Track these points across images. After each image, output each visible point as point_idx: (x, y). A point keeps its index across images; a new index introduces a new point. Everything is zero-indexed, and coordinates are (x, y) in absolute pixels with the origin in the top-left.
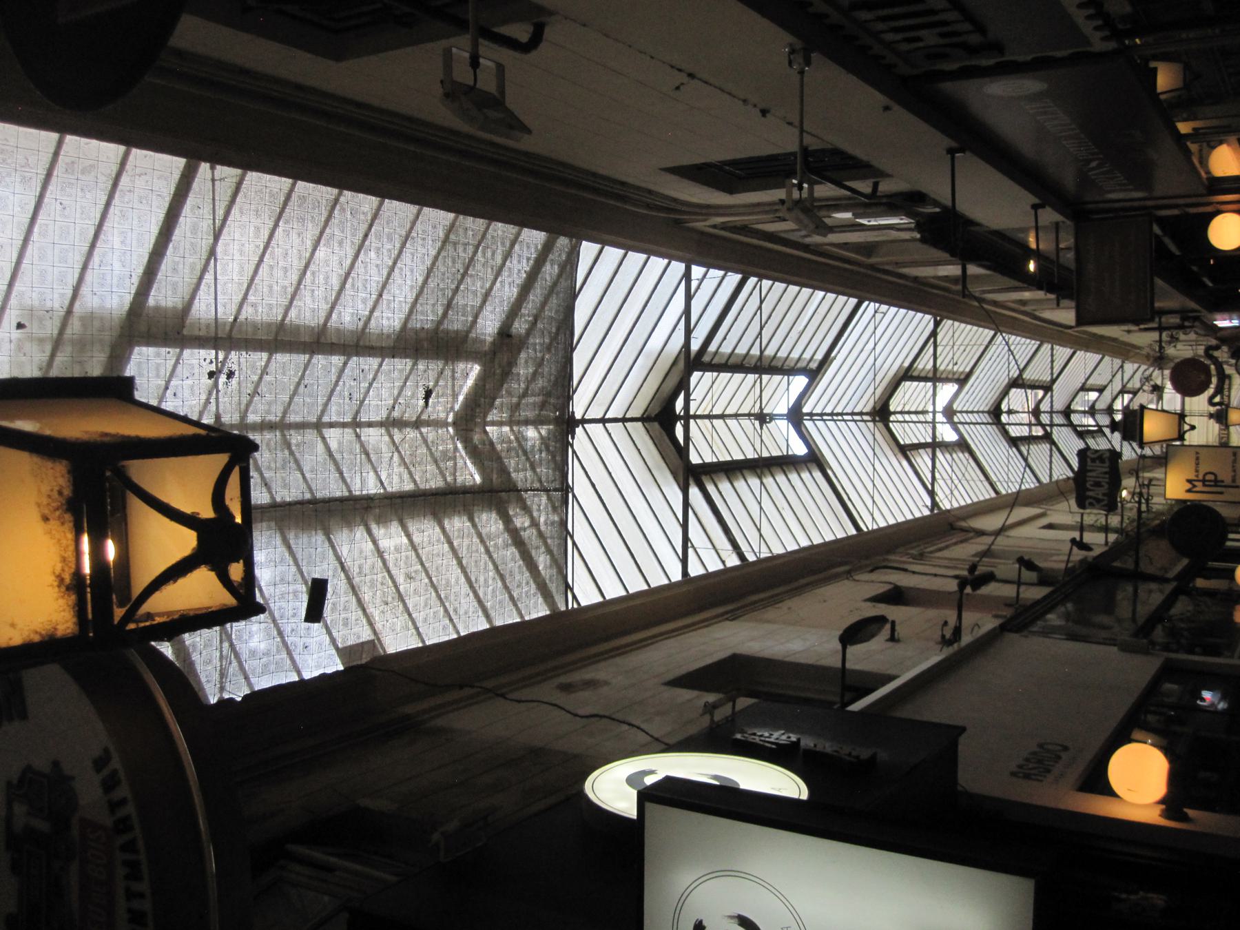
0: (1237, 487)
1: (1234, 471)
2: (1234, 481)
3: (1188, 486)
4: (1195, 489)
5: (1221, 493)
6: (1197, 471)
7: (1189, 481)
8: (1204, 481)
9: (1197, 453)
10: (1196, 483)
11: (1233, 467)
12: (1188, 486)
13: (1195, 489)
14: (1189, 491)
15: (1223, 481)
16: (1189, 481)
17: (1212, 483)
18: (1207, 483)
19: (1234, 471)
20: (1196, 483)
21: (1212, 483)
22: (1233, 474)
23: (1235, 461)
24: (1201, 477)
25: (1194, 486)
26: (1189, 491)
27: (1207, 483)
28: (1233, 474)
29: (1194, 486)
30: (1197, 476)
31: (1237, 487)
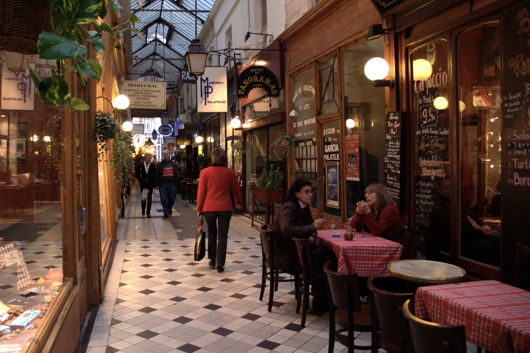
0: (206, 104)
2: (209, 102)
5: (202, 96)
6: (213, 83)
9: (223, 83)
11: (217, 102)
15: (208, 97)
19: (214, 102)
24: (209, 85)
25: (204, 82)
29: (204, 82)
31: (206, 104)
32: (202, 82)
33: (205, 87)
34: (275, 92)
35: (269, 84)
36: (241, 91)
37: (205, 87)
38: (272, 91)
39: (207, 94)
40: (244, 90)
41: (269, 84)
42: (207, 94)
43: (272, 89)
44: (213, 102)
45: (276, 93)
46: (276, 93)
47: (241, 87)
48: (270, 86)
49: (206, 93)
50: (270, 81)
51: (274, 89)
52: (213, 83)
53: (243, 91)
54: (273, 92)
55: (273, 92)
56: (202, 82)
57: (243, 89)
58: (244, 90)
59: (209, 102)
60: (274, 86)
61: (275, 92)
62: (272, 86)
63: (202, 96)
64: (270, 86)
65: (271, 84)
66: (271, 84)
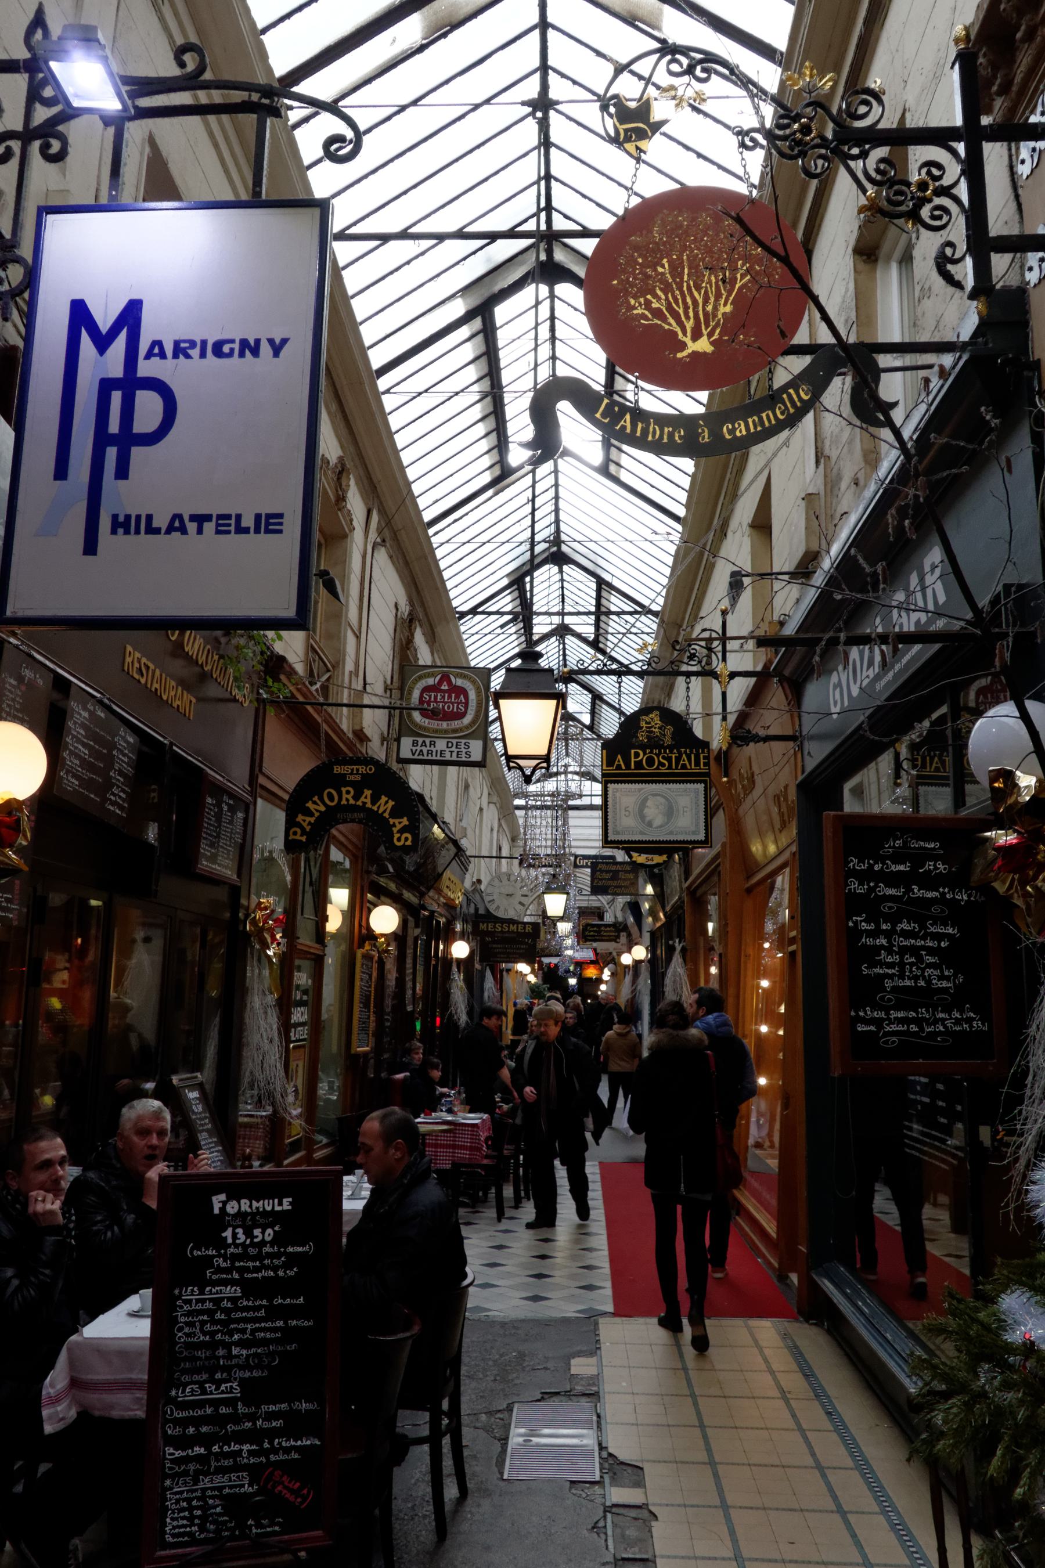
0: (90, 547)
1: (177, 525)
2: (122, 525)
3: (104, 317)
4: (86, 341)
5: (61, 471)
6: (179, 350)
9: (277, 349)
10: (119, 345)
11: (201, 519)
12: (104, 317)
13: (86, 341)
14: (80, 313)
15: (122, 472)
17: (114, 427)
18: (116, 397)
19: (177, 525)
20: (119, 345)
21: (114, 427)
24: (145, 368)
25: (102, 343)
26: (80, 313)
27: (116, 397)
28: (161, 521)
29: (102, 343)
30: (157, 349)
31: (90, 547)
32: (85, 339)
33: (106, 386)
34: (406, 839)
35: (386, 815)
36: (299, 831)
37: (106, 386)
38: (397, 836)
39: (112, 453)
40: (308, 828)
41: (386, 815)
42: (111, 453)
43: (395, 830)
44: (161, 521)
45: (409, 843)
46: (409, 843)
47: (300, 818)
48: (391, 821)
49: (102, 439)
50: (391, 803)
51: (401, 831)
52: (179, 350)
53: (304, 832)
54: (399, 839)
55: (399, 839)
56: (85, 339)
57: (305, 825)
58: (308, 828)
59: (122, 525)
60: (405, 821)
61: (406, 839)
62: (396, 821)
63: (61, 471)
64: (391, 821)
65: (395, 813)
66: (395, 813)
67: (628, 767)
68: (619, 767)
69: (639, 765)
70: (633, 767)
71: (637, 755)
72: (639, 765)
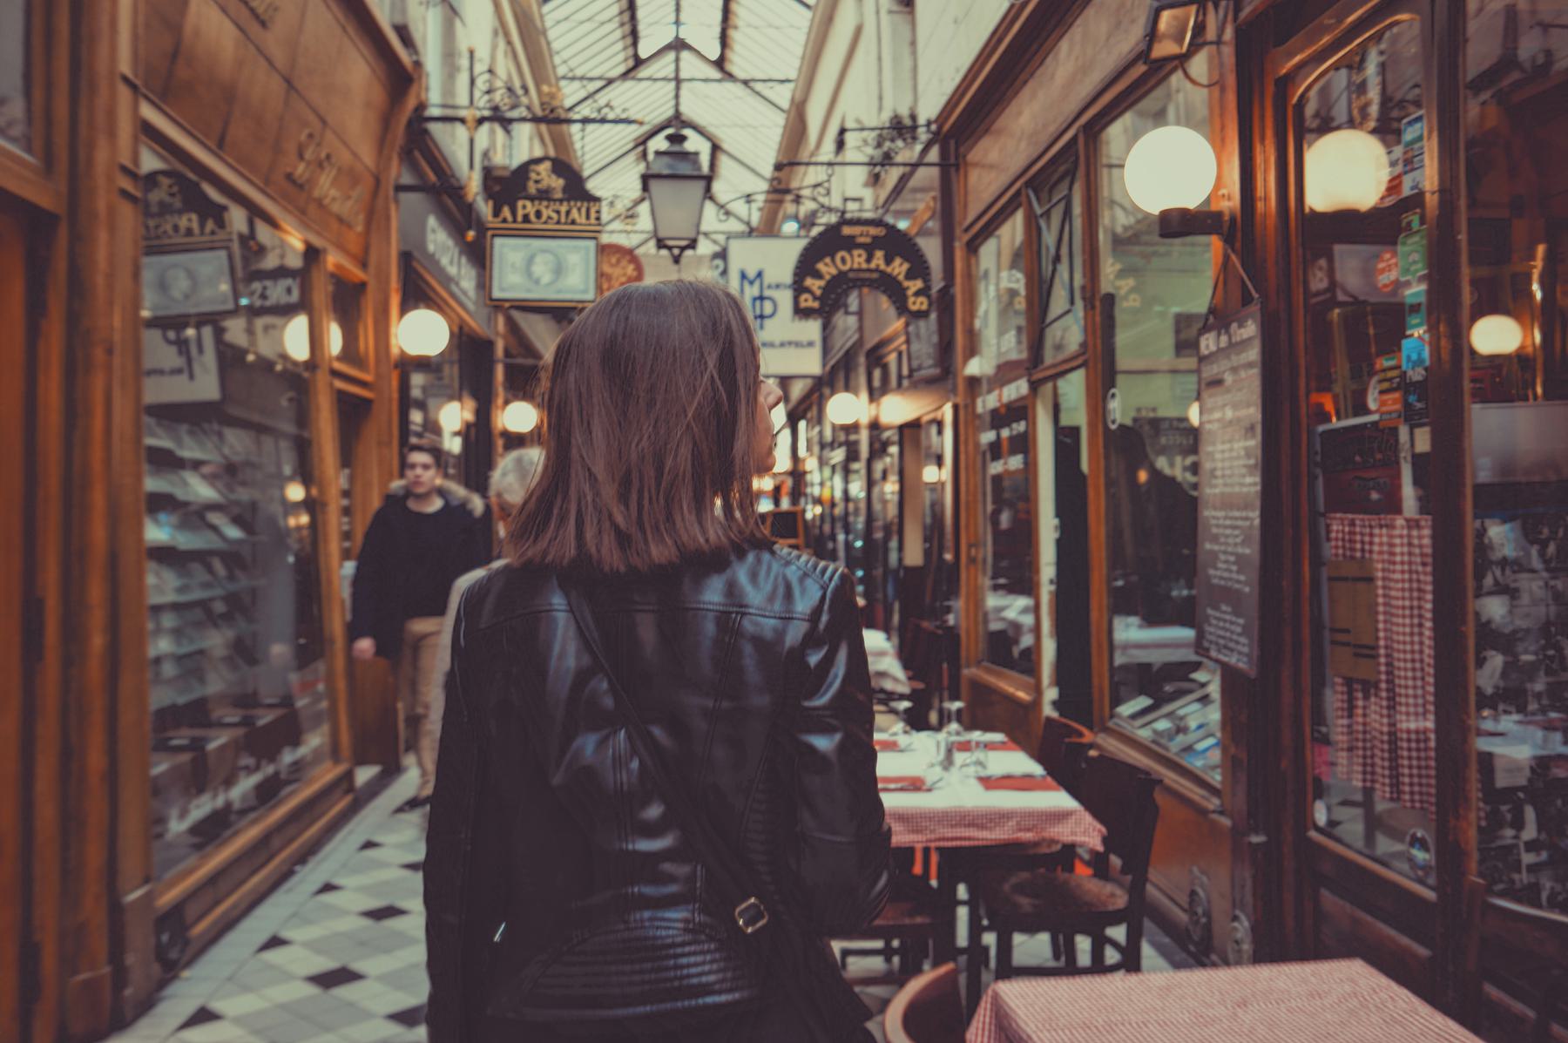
1: (782, 345)
3: (751, 274)
6: (778, 286)
7: (760, 275)
8: (761, 298)
12: (751, 274)
14: (743, 276)
16: (760, 275)
18: (758, 303)
19: (782, 345)
22: (777, 342)
23: (798, 344)
24: (767, 293)
25: (751, 283)
26: (743, 276)
29: (751, 283)
30: (769, 287)
52: (778, 286)
67: (515, 221)
68: (505, 221)
69: (526, 219)
70: (520, 218)
71: (524, 207)
72: (526, 219)
